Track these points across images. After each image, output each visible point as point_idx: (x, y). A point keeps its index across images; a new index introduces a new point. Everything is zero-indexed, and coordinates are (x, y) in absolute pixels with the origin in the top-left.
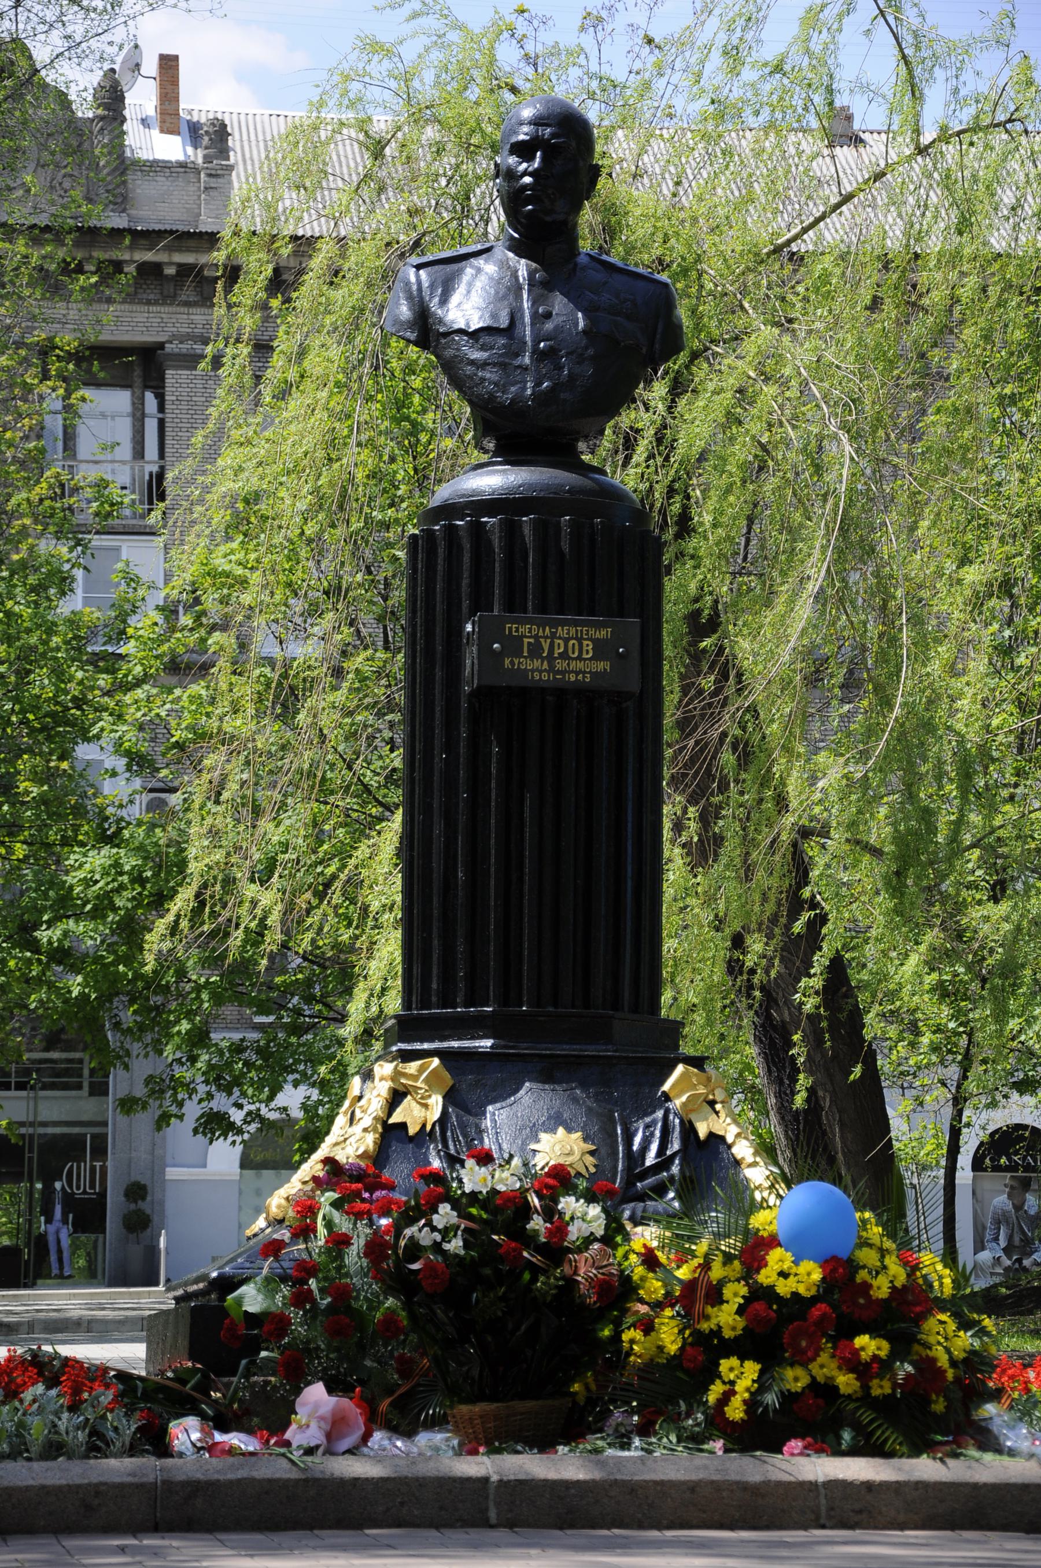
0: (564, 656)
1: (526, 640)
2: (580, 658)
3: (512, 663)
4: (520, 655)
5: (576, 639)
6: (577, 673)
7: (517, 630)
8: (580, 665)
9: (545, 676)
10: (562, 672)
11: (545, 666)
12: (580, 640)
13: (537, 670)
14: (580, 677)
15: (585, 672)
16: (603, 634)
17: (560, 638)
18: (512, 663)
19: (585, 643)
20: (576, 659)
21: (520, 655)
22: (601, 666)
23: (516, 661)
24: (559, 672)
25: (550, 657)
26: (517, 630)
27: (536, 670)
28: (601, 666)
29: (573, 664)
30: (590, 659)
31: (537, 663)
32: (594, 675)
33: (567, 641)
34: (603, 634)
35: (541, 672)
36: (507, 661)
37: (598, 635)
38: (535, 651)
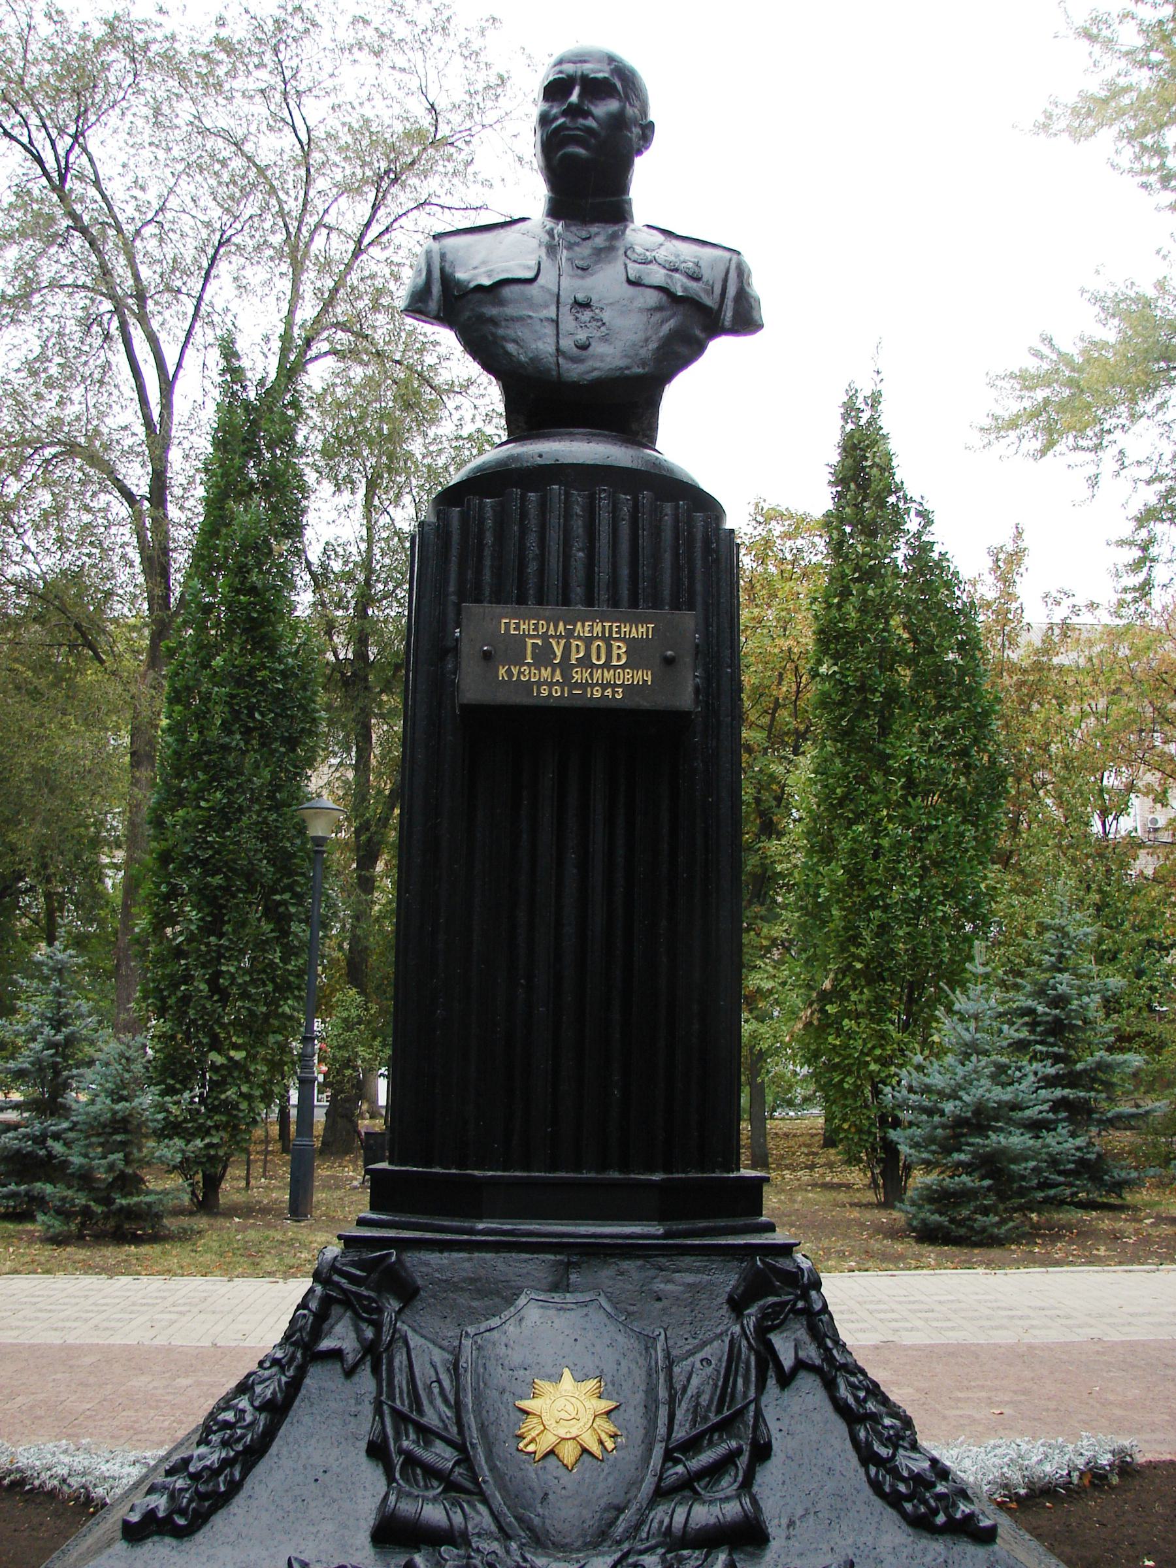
0: (585, 663)
1: (530, 642)
2: (607, 666)
3: (509, 672)
4: (520, 661)
5: (603, 638)
6: (604, 687)
7: (517, 625)
8: (608, 675)
9: (557, 692)
10: (583, 686)
11: (558, 677)
12: (608, 640)
13: (545, 683)
16: (641, 631)
17: (579, 638)
18: (509, 672)
21: (520, 661)
22: (642, 676)
23: (515, 671)
24: (577, 685)
25: (565, 666)
26: (517, 628)
27: (545, 683)
28: (642, 676)
29: (598, 674)
30: (622, 667)
31: (546, 673)
32: (629, 689)
33: (588, 641)
34: (641, 631)
35: (551, 685)
36: (502, 671)
37: (634, 634)
38: (543, 656)
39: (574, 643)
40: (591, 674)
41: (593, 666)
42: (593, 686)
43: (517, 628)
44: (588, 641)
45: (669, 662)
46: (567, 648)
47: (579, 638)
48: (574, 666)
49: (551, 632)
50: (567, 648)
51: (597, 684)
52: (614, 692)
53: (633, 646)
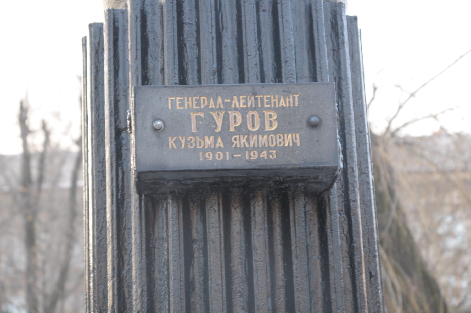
1: (193, 116)
2: (261, 131)
3: (177, 142)
6: (260, 149)
8: (263, 140)
9: (219, 156)
10: (243, 150)
12: (261, 110)
14: (264, 154)
15: (270, 148)
17: (236, 109)
18: (177, 142)
19: (267, 114)
20: (258, 133)
25: (225, 134)
26: (182, 104)
30: (275, 132)
31: (209, 141)
32: (283, 150)
35: (214, 150)
36: (171, 142)
38: (207, 127)
39: (232, 114)
40: (248, 140)
41: (248, 133)
42: (250, 149)
43: (182, 104)
44: (244, 112)
45: (314, 126)
46: (226, 119)
47: (236, 109)
48: (234, 134)
49: (212, 105)
50: (226, 119)
51: (254, 148)
52: (268, 154)
53: (282, 112)
